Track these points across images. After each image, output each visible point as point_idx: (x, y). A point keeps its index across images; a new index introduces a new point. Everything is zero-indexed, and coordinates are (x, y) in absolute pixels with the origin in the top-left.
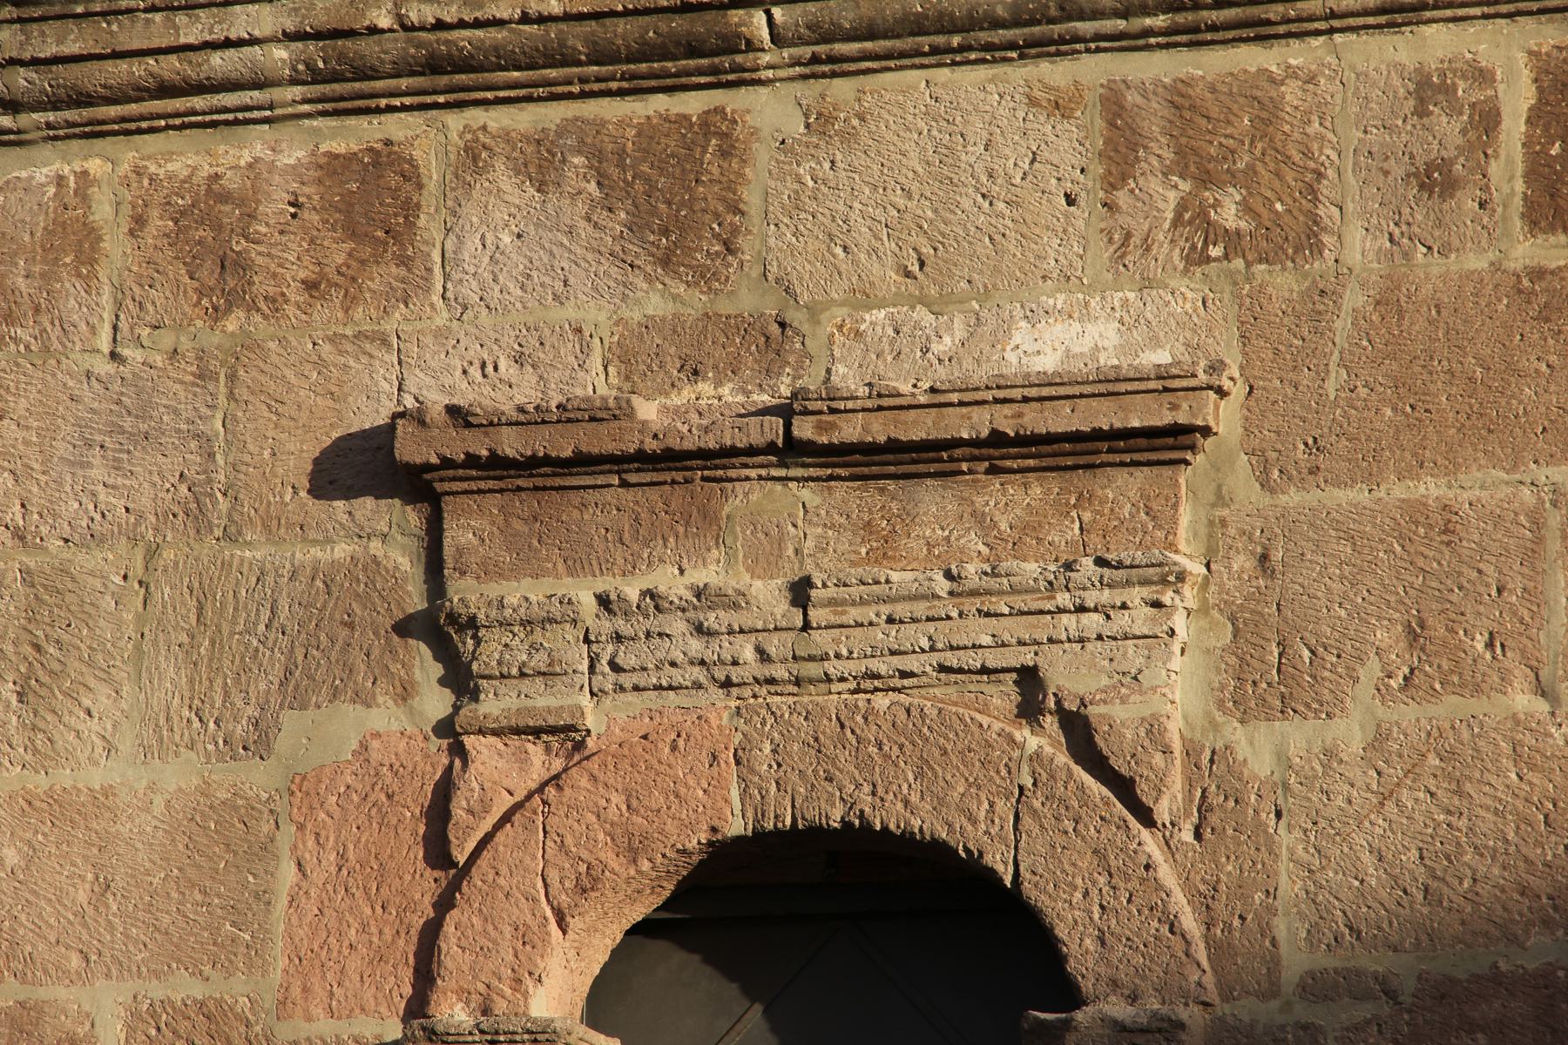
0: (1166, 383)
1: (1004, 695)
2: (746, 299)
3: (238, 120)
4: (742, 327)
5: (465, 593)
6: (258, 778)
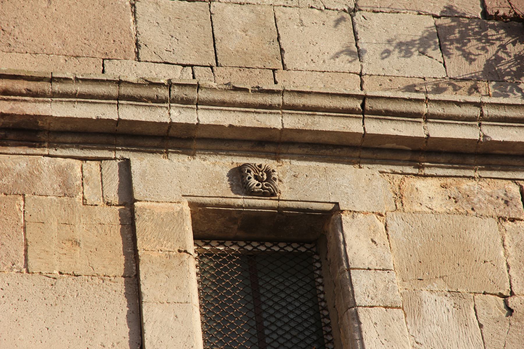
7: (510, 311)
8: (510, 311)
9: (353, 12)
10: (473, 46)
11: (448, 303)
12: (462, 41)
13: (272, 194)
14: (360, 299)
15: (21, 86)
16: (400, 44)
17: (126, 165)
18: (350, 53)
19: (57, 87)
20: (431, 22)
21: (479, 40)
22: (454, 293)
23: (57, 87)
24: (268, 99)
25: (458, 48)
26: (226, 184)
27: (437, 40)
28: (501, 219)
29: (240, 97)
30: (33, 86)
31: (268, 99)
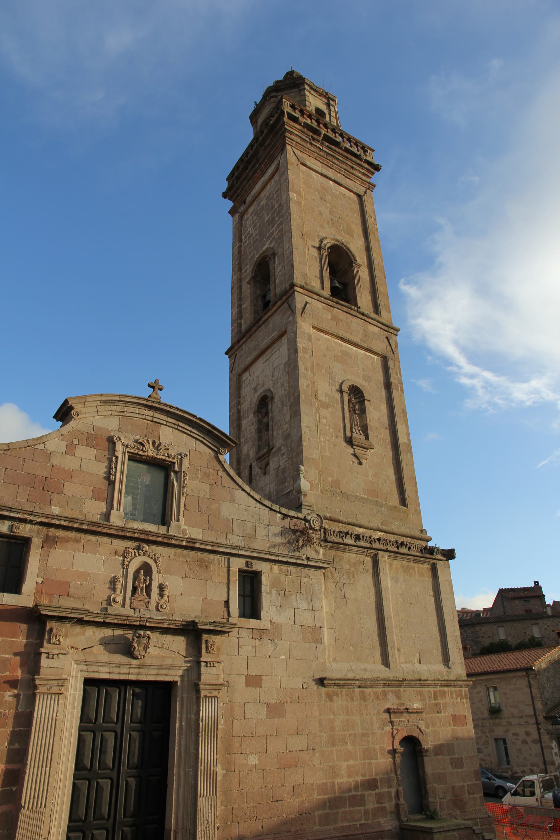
0: (421, 709)
1: (416, 727)
2: (402, 702)
3: (378, 688)
4: (402, 703)
5: (392, 720)
6: (383, 731)
7: (285, 595)
8: (285, 595)
9: (268, 525)
10: (287, 535)
11: (276, 592)
12: (285, 534)
13: (251, 568)
14: (263, 591)
15: (216, 545)
17: (229, 559)
18: (266, 535)
19: (222, 545)
20: (280, 529)
22: (277, 590)
23: (222, 545)
24: (255, 551)
26: (244, 565)
28: (286, 575)
29: (250, 550)
30: (218, 545)
31: (255, 551)
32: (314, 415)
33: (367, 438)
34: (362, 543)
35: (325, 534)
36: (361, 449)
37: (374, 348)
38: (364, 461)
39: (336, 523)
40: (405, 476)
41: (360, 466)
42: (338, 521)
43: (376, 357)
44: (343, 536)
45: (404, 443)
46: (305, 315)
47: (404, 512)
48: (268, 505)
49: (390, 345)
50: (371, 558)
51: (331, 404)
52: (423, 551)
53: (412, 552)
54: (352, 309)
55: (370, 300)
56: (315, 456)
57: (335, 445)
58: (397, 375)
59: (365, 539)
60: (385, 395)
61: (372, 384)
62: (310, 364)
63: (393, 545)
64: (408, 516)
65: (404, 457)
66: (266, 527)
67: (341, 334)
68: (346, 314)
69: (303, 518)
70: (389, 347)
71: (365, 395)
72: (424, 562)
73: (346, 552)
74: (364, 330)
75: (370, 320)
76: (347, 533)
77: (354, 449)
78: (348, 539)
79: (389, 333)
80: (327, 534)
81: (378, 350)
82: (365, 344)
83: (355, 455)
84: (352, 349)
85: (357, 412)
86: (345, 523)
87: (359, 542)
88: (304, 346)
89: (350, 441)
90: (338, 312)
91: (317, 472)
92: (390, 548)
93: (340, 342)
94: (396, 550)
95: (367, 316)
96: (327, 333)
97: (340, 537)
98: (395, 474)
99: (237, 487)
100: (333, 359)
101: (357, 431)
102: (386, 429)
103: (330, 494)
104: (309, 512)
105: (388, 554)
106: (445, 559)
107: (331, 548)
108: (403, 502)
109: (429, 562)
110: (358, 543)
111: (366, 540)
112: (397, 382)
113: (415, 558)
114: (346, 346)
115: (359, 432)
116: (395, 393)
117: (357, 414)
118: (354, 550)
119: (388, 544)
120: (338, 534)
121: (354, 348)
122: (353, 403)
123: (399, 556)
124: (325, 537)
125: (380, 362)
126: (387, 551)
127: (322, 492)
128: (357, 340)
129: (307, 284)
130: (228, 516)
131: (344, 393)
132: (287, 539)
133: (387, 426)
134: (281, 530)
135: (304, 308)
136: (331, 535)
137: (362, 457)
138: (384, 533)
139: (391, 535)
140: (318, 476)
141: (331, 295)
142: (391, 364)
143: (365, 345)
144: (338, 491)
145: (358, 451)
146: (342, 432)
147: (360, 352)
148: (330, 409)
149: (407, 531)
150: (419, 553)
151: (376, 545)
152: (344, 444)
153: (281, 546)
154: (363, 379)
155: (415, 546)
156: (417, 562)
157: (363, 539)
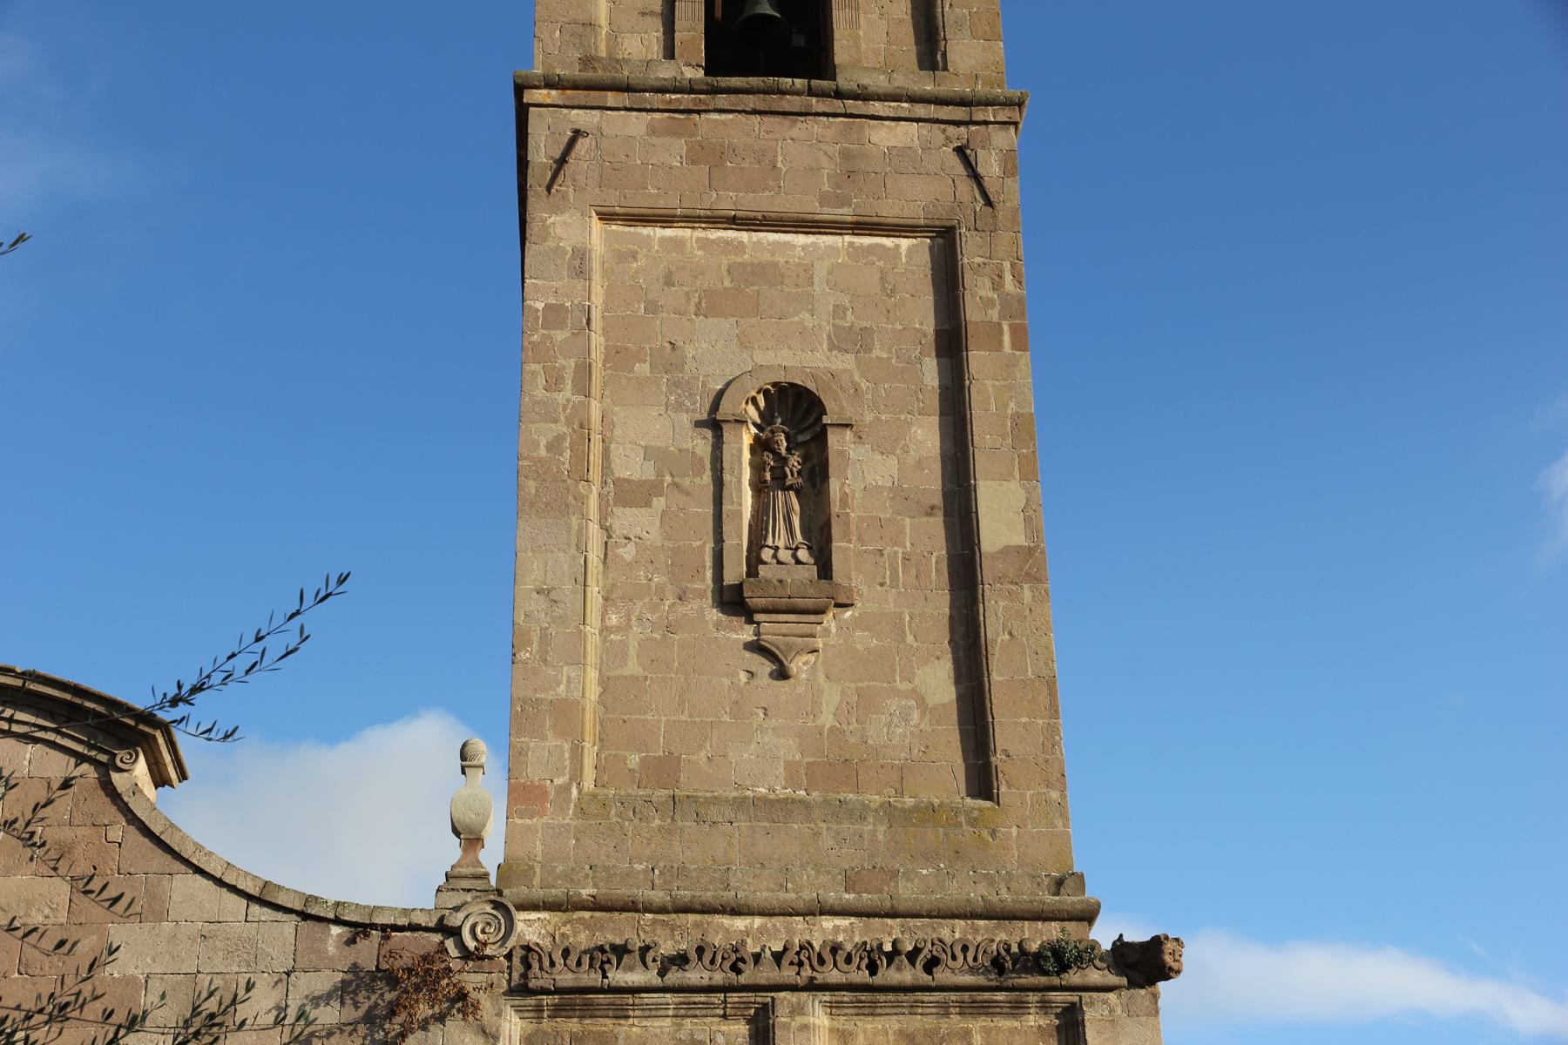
9: (288, 974)
12: (355, 993)
16: (314, 998)
20: (339, 977)
21: (367, 990)
25: (352, 999)
27: (340, 993)
32: (574, 541)
33: (825, 570)
34: (695, 975)
35: (528, 966)
36: (792, 617)
37: (889, 210)
38: (797, 665)
39: (625, 915)
40: (995, 677)
41: (781, 683)
42: (631, 907)
43: (905, 243)
44: (609, 961)
45: (1006, 551)
46: (564, 186)
47: (973, 822)
48: (289, 905)
49: (976, 177)
50: (748, 1022)
51: (668, 479)
52: (1009, 965)
53: (942, 976)
54: (782, 93)
55: (908, 18)
56: (562, 687)
57: (669, 628)
58: (997, 283)
59: (707, 957)
60: (936, 383)
61: (877, 352)
62: (572, 363)
63: (849, 960)
64: (993, 833)
65: (996, 612)
66: (280, 980)
67: (728, 202)
68: (756, 119)
69: (431, 925)
70: (966, 188)
71: (829, 404)
72: (1018, 1008)
73: (627, 1017)
74: (846, 155)
75: (877, 108)
76: (621, 951)
77: (758, 623)
78: (631, 969)
79: (973, 128)
80: (536, 965)
81: (913, 212)
82: (845, 210)
83: (757, 647)
84: (787, 243)
85: (790, 481)
86: (662, 910)
87: (680, 974)
88: (552, 301)
89: (733, 601)
90: (724, 123)
91: (567, 746)
92: (833, 976)
93: (730, 234)
94: (863, 976)
95: (856, 97)
96: (666, 220)
97: (591, 966)
98: (957, 682)
99: (178, 866)
100: (693, 308)
101: (785, 555)
102: (931, 515)
103: (619, 815)
104: (469, 897)
105: (827, 996)
106: (1124, 981)
107: (558, 1011)
108: (982, 782)
109: (1045, 1006)
110: (674, 977)
111: (712, 962)
112: (994, 314)
113: (966, 996)
114: (759, 243)
115: (794, 556)
116: (977, 360)
117: (791, 488)
118: (658, 1007)
119: (822, 961)
120: (586, 959)
121: (801, 240)
122: (776, 453)
123: (882, 997)
124: (524, 976)
125: (925, 258)
126: (812, 987)
127: (581, 811)
128: (812, 207)
129: (587, 61)
130: (131, 971)
131: (725, 427)
132: (365, 1007)
133: (938, 500)
134: (343, 981)
135: (562, 162)
136: (552, 964)
137: (790, 647)
138: (853, 919)
139: (889, 921)
140: (572, 757)
141: (710, 70)
142: (971, 252)
143: (845, 213)
144: (661, 794)
145: (773, 629)
146: (709, 574)
147: (828, 247)
148: (659, 503)
149: (977, 894)
150: (987, 971)
151: (767, 973)
152: (714, 615)
153: (337, 1035)
154: (832, 347)
155: (965, 949)
156: (984, 1009)
157: (700, 959)
